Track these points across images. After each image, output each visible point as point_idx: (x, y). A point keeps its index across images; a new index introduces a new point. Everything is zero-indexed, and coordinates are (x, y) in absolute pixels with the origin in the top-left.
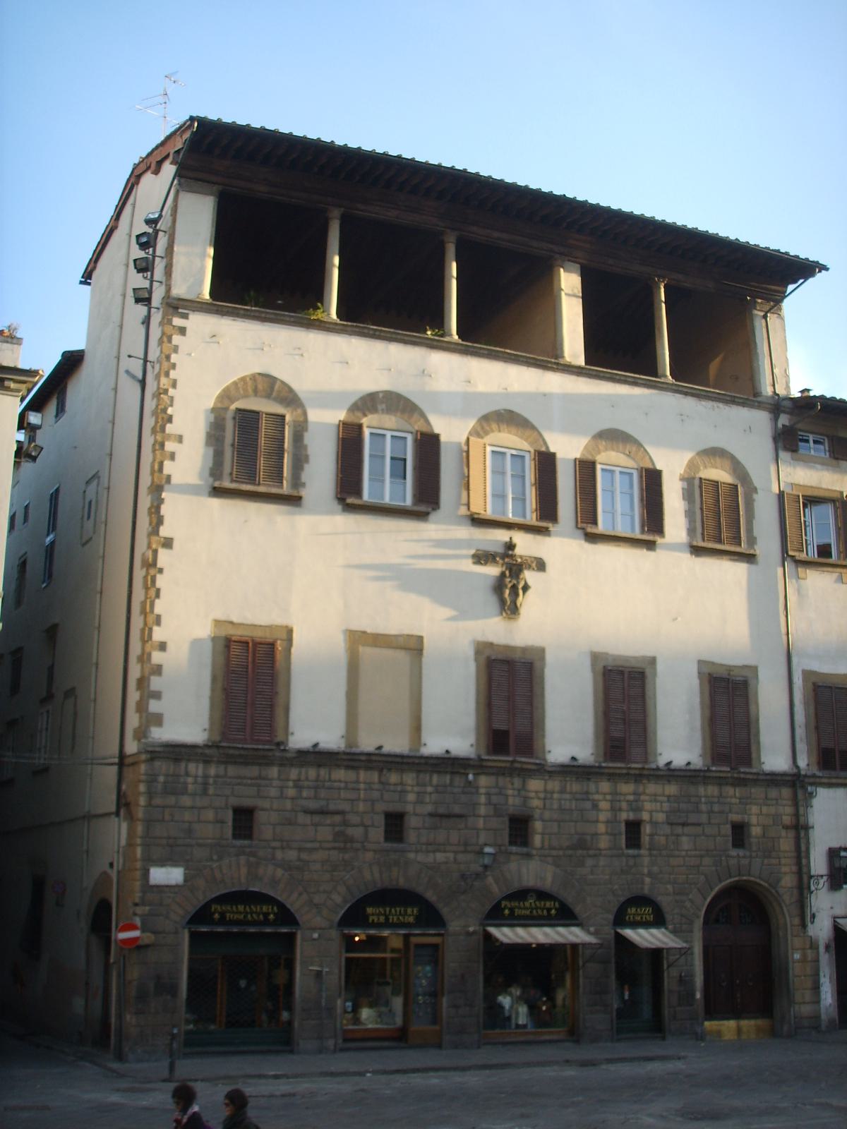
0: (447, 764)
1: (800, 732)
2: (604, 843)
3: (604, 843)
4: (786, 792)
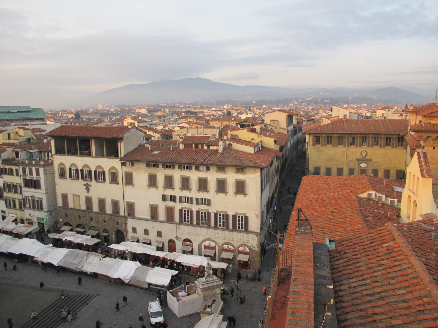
0: (83, 211)
1: (126, 210)
2: (101, 222)
3: (101, 222)
4: (124, 218)
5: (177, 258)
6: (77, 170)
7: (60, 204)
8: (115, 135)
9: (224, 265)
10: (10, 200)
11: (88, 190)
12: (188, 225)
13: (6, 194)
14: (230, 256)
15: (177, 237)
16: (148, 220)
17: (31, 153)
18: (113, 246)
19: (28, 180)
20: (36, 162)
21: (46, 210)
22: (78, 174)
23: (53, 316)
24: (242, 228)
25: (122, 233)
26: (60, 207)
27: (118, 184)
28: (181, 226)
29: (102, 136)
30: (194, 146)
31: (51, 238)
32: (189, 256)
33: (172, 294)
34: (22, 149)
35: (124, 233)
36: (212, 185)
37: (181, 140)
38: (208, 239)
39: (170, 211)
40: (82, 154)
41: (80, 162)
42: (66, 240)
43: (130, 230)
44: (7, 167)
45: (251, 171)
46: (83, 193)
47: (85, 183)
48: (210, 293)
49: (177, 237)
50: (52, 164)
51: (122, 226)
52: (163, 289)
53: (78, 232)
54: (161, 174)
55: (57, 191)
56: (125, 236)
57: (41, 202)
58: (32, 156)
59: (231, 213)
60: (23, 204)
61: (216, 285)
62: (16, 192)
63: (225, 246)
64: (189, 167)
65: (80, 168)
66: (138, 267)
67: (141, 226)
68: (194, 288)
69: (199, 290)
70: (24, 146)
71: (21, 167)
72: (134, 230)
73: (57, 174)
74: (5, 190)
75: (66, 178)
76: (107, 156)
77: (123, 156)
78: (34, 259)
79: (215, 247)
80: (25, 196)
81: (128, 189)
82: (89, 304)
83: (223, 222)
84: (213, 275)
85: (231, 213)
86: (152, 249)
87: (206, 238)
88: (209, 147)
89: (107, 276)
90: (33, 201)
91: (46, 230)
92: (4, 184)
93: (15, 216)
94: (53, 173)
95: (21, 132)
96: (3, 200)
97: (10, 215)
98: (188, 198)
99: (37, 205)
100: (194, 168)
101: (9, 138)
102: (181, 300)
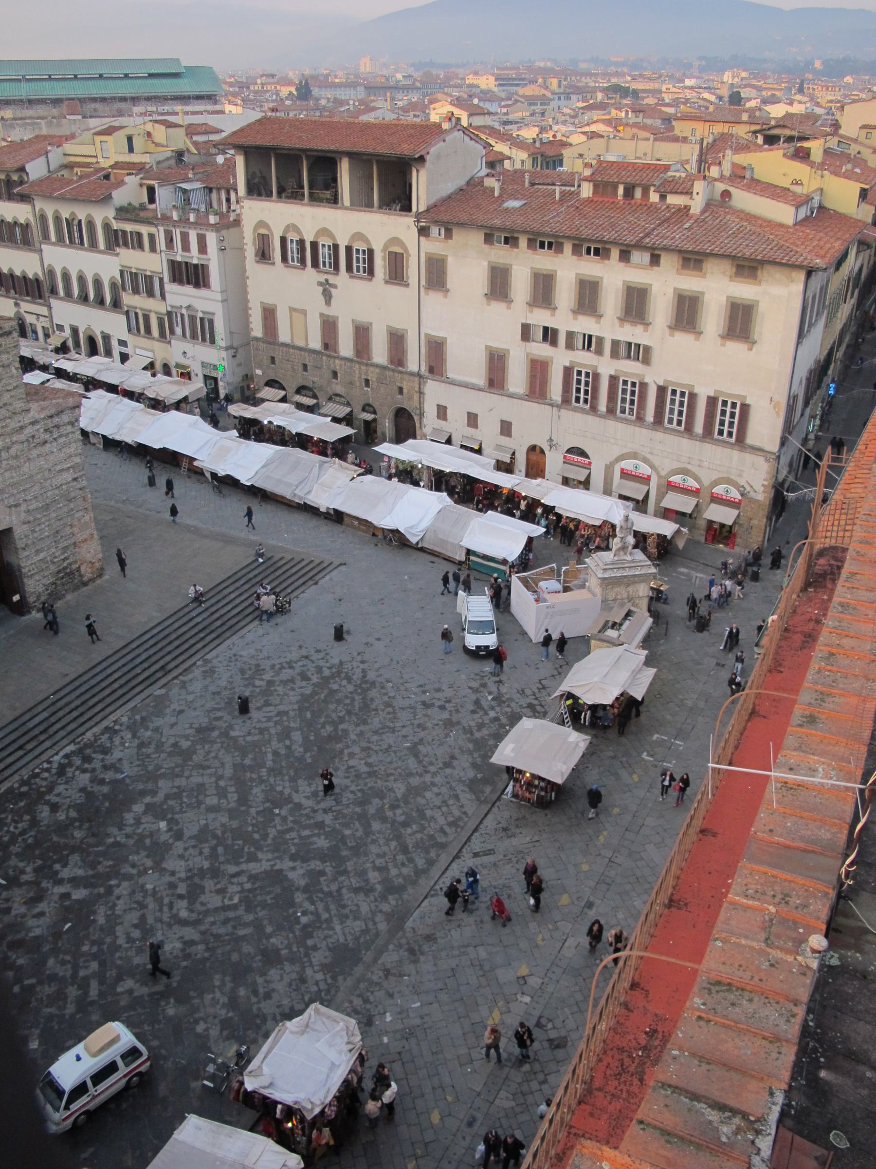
0: (314, 352)
2: (358, 384)
3: (358, 384)
4: (417, 379)
5: (546, 495)
6: (301, 243)
7: (257, 331)
8: (405, 149)
9: (667, 528)
10: (136, 314)
11: (328, 297)
12: (583, 411)
13: (128, 299)
14: (686, 504)
15: (551, 440)
16: (480, 390)
17: (185, 191)
18: (386, 449)
19: (180, 263)
20: (198, 217)
21: (223, 344)
22: (307, 254)
23: (237, 601)
24: (730, 434)
25: (410, 417)
26: (257, 339)
27: (407, 285)
28: (564, 412)
29: (370, 150)
30: (621, 190)
31: (235, 417)
32: (579, 494)
33: (525, 582)
34: (165, 181)
35: (416, 418)
36: (661, 308)
37: (588, 172)
38: (634, 455)
39: (538, 371)
40: (314, 199)
41: (307, 219)
42: (270, 422)
43: (430, 410)
44: (129, 227)
45: (778, 276)
46: (316, 307)
47: (322, 278)
48: (622, 592)
49: (551, 440)
50: (237, 223)
51: (410, 398)
52: (502, 567)
53: (300, 406)
54: (523, 263)
55: (249, 297)
56: (418, 425)
57: (211, 322)
58: (187, 201)
59: (703, 392)
60: (167, 327)
61: (641, 575)
62: (150, 293)
63: (676, 479)
64: (600, 252)
65: (309, 238)
66: (445, 508)
67: (460, 403)
68: (582, 576)
69: (593, 583)
70: (167, 171)
71: (161, 229)
72: (442, 413)
73: (250, 252)
74: (124, 289)
75: (274, 264)
76: (380, 207)
77: (422, 208)
78: (195, 463)
79: (649, 478)
80: (172, 307)
81: (432, 299)
82: (320, 582)
83: (680, 413)
84: (635, 547)
85: (703, 392)
86: (483, 466)
87: (628, 450)
88: (663, 197)
89: (366, 521)
90: (192, 318)
91: (222, 396)
92: (122, 272)
93: (150, 354)
94: (241, 250)
95: (160, 133)
96: (121, 313)
97: (138, 351)
98: (590, 337)
99: (202, 330)
100: (615, 253)
101: (131, 150)
102: (545, 601)
